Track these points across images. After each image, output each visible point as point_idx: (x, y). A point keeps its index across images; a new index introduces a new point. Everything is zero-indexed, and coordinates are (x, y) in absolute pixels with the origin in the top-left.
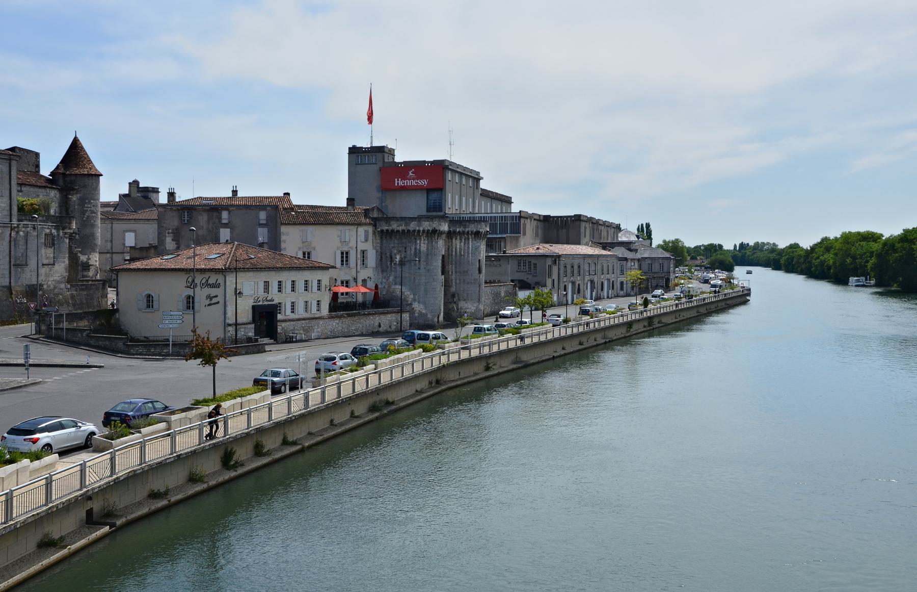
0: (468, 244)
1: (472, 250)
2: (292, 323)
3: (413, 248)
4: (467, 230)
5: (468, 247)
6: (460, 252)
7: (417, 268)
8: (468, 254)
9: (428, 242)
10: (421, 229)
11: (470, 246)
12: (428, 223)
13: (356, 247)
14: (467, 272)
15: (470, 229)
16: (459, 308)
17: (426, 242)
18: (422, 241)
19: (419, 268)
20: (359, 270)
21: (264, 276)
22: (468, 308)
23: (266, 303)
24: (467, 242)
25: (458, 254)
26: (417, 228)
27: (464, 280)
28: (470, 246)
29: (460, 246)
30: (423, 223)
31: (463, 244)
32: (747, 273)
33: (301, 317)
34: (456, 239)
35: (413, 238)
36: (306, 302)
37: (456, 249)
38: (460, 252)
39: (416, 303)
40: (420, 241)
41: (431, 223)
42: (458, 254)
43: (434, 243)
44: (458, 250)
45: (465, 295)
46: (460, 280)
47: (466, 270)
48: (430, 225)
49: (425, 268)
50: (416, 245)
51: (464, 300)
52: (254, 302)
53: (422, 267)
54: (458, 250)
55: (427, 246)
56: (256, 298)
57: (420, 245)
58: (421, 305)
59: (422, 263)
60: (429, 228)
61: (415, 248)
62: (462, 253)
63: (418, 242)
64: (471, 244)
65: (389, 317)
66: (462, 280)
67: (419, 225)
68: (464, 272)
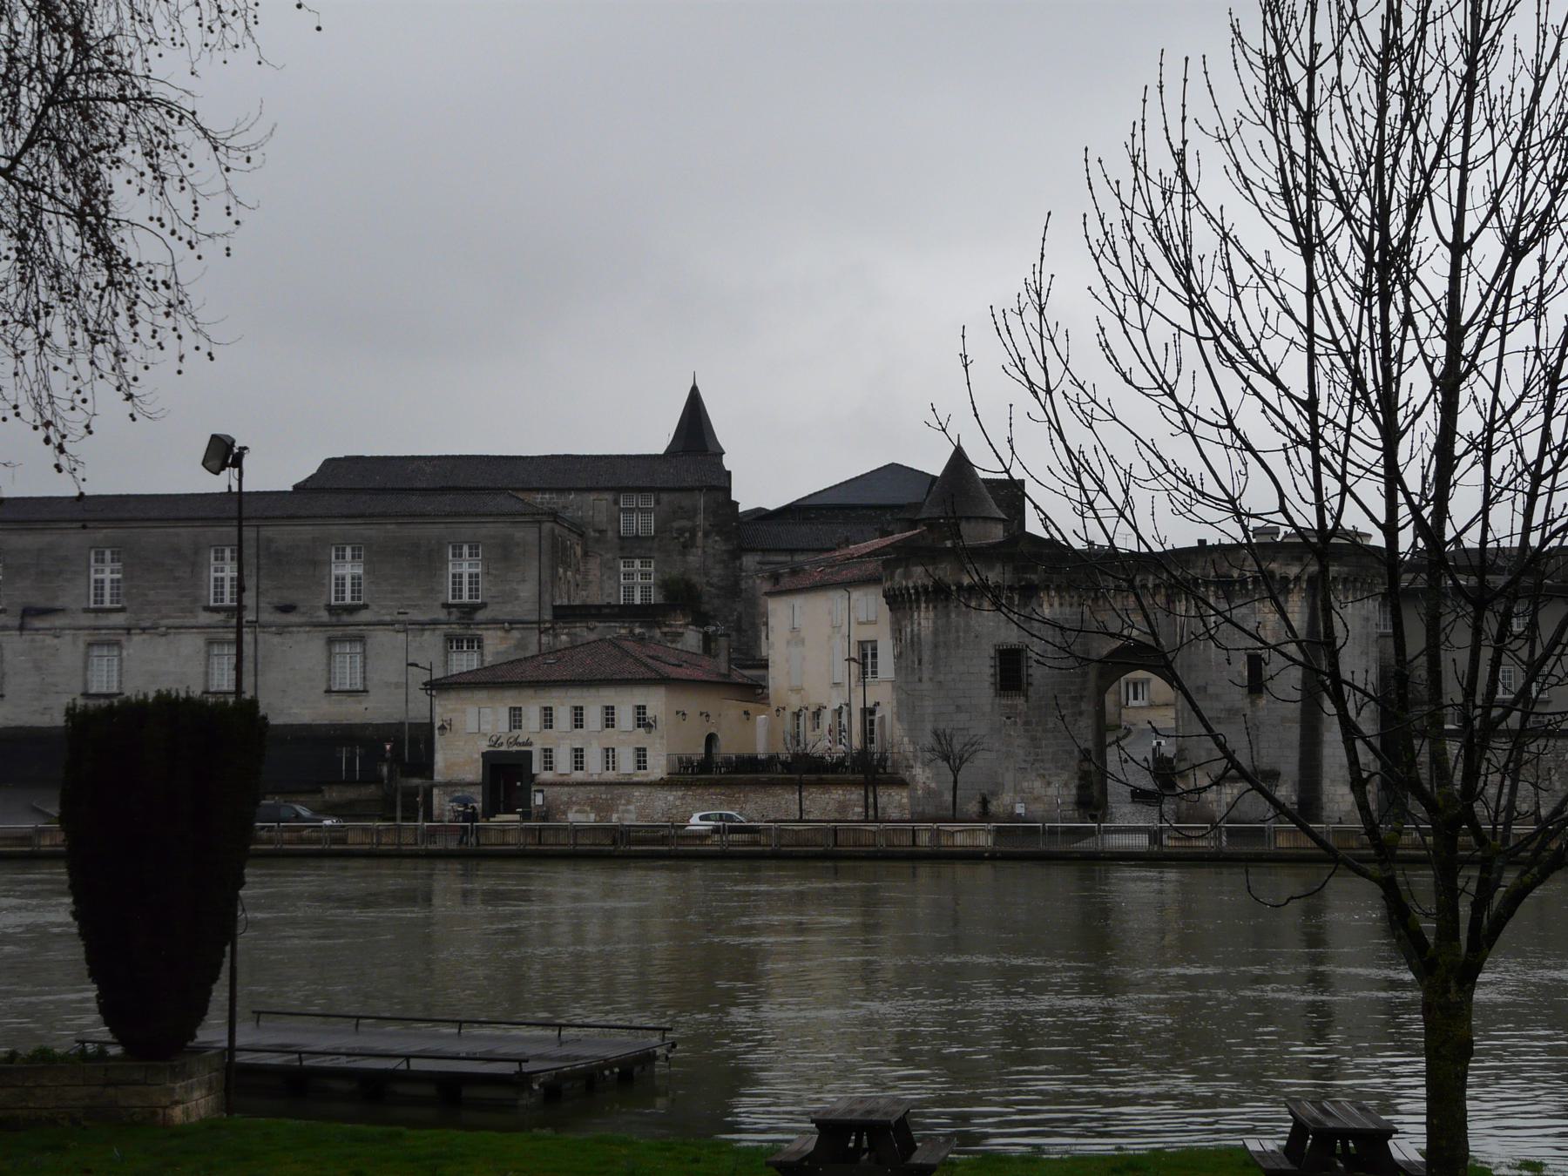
2: (566, 789)
3: (909, 630)
9: (936, 616)
10: (911, 585)
14: (1205, 688)
17: (931, 614)
18: (922, 614)
19: (920, 680)
20: (853, 685)
21: (510, 698)
23: (515, 748)
30: (914, 568)
33: (595, 778)
36: (607, 750)
39: (919, 765)
40: (919, 616)
41: (931, 569)
43: (953, 616)
49: (931, 679)
50: (912, 624)
52: (490, 746)
53: (926, 677)
55: (934, 623)
56: (494, 739)
57: (919, 624)
58: (928, 771)
61: (912, 630)
63: (916, 614)
65: (837, 794)
67: (907, 576)
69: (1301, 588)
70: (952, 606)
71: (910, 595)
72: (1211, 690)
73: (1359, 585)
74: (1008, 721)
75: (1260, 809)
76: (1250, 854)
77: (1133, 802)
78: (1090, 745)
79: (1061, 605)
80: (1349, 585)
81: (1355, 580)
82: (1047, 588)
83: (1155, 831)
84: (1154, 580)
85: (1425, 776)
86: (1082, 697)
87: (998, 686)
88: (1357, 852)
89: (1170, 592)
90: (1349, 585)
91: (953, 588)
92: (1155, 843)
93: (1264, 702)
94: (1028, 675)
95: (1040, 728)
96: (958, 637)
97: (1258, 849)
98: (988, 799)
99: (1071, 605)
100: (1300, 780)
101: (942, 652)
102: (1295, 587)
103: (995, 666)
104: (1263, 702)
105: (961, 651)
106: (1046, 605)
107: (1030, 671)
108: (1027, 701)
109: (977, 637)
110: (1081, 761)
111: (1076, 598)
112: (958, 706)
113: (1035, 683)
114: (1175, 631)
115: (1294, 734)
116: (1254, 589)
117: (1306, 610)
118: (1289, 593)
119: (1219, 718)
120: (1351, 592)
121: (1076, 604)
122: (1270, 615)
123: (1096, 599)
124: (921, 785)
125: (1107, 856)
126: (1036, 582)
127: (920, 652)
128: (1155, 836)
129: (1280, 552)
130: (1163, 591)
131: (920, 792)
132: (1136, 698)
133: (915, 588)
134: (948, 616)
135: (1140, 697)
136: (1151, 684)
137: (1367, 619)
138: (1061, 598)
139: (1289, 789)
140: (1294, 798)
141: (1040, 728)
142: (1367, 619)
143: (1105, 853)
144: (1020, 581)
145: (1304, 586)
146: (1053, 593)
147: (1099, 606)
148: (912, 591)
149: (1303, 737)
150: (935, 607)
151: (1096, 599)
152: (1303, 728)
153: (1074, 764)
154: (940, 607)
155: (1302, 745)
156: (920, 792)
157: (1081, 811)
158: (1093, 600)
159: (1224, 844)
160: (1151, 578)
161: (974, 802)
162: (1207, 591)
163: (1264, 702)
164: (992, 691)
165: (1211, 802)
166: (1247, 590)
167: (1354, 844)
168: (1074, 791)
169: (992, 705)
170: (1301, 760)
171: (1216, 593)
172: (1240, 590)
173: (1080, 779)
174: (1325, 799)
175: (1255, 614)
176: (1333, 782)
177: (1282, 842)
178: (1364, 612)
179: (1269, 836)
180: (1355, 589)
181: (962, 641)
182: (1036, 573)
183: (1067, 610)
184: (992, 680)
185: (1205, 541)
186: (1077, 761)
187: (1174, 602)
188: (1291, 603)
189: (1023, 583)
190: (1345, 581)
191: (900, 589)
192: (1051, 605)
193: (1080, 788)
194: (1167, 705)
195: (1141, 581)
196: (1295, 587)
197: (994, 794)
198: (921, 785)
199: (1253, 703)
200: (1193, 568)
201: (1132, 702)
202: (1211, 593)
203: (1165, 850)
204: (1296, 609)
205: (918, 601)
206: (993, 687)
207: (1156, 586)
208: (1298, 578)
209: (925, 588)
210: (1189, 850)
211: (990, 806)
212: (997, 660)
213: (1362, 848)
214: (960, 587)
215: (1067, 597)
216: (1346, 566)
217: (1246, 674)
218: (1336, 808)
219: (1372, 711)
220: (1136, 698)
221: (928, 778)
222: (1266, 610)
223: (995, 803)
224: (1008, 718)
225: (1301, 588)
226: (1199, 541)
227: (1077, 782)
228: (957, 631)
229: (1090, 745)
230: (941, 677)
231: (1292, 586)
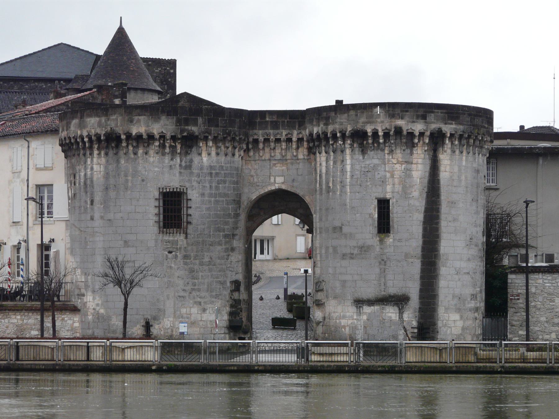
0: (343, 161)
1: (352, 176)
3: (82, 174)
4: (330, 128)
5: (343, 171)
6: (327, 183)
7: (89, 218)
8: (343, 187)
9: (107, 161)
10: (85, 134)
11: (348, 168)
12: (98, 119)
13: (28, 180)
14: (341, 228)
15: (337, 127)
16: (326, 315)
17: (103, 160)
18: (95, 160)
19: (92, 219)
20: (31, 224)
22: (344, 317)
24: (340, 158)
25: (324, 187)
26: (79, 132)
27: (335, 249)
28: (348, 168)
29: (327, 167)
30: (88, 120)
31: (331, 163)
32: (52, 185)
34: (320, 153)
35: (82, 152)
37: (321, 176)
38: (327, 183)
39: (90, 293)
40: (92, 160)
41: (103, 119)
42: (324, 187)
43: (122, 161)
44: (324, 176)
45: (338, 284)
46: (327, 248)
47: (337, 224)
48: (100, 124)
49: (102, 218)
50: (85, 169)
51: (335, 298)
53: (97, 215)
54: (324, 176)
55: (106, 168)
57: (92, 169)
58: (97, 298)
59: (97, 206)
60: (98, 131)
61: (85, 175)
62: (331, 185)
63: (89, 161)
64: (348, 162)
65: (16, 319)
66: (331, 250)
67: (81, 126)
68: (335, 228)
69: (424, 143)
70: (121, 153)
71: (84, 143)
72: (345, 230)
73: (471, 141)
74: (170, 255)
75: (386, 332)
76: (384, 366)
77: (274, 328)
78: (240, 277)
79: (218, 154)
80: (464, 142)
81: (469, 137)
82: (206, 139)
83: (303, 348)
84: (298, 134)
85: (522, 305)
86: (234, 235)
87: (162, 224)
88: (474, 365)
89: (311, 145)
90: (464, 142)
91: (123, 137)
92: (303, 357)
93: (391, 240)
94: (187, 215)
95: (197, 262)
96: (127, 181)
97: (390, 362)
98: (150, 323)
99: (226, 155)
100: (420, 308)
101: (112, 194)
102: (419, 141)
103: (159, 207)
104: (389, 240)
105: (129, 192)
106: (204, 154)
107: (190, 211)
108: (186, 238)
109: (143, 180)
110: (232, 291)
111: (230, 149)
112: (126, 242)
113: (194, 222)
114: (316, 179)
115: (416, 267)
116: (385, 142)
117: (428, 162)
118: (414, 147)
119: (353, 254)
120: (465, 146)
121: (230, 154)
122: (397, 166)
123: (247, 150)
124: (91, 311)
125: (260, 368)
126: (197, 134)
127: (92, 194)
128: (303, 352)
129: (407, 111)
130: (305, 144)
131: (90, 317)
132: (262, 252)
133: (89, 137)
134: (118, 162)
135: (266, 252)
136: (275, 240)
137: (478, 171)
138: (218, 148)
139: (411, 315)
140: (415, 324)
141: (197, 262)
142: (478, 171)
143: (259, 366)
144: (182, 131)
145: (427, 141)
146: (210, 143)
147: (250, 157)
148: (86, 140)
149: (423, 271)
150: (106, 154)
151: (247, 150)
152: (423, 263)
153: (226, 293)
154: (111, 153)
155: (422, 278)
156: (90, 317)
157: (232, 334)
158: (245, 151)
159: (361, 359)
160: (295, 132)
161: (138, 326)
162: (344, 143)
163: (391, 240)
164: (156, 229)
165: (344, 327)
166: (379, 143)
167: (472, 358)
168: (226, 317)
169: (156, 241)
170: (421, 291)
171: (352, 146)
172: (373, 143)
173: (232, 306)
174: (440, 324)
175: (385, 164)
176: (447, 309)
177: (411, 357)
178: (475, 165)
179: (401, 350)
180: (468, 145)
181: (130, 184)
182: (196, 124)
183: (222, 158)
184: (156, 219)
185: (342, 101)
186: (229, 291)
187: (314, 154)
188: (415, 156)
189: (185, 134)
190: (461, 137)
191: (75, 138)
192: (209, 154)
193: (231, 314)
194: (288, 259)
195: (286, 135)
196: (419, 141)
197: (155, 318)
198: (91, 311)
199: (381, 241)
200: (333, 124)
201: (259, 256)
202: (347, 146)
203: (310, 364)
204: (420, 161)
205: (91, 148)
206: (157, 225)
207: (300, 140)
208: (422, 134)
209: (98, 136)
210: (333, 364)
211: (152, 329)
212: (161, 201)
213: (478, 362)
214: (129, 136)
215: (223, 148)
216: (461, 124)
217: (376, 216)
218: (449, 332)
219: (480, 250)
220: (262, 252)
221: (98, 305)
222: (395, 161)
223: (157, 327)
224: (170, 252)
225: (424, 143)
226: (337, 102)
227: (228, 309)
228: (126, 176)
229: (240, 277)
230: (111, 216)
231: (416, 141)
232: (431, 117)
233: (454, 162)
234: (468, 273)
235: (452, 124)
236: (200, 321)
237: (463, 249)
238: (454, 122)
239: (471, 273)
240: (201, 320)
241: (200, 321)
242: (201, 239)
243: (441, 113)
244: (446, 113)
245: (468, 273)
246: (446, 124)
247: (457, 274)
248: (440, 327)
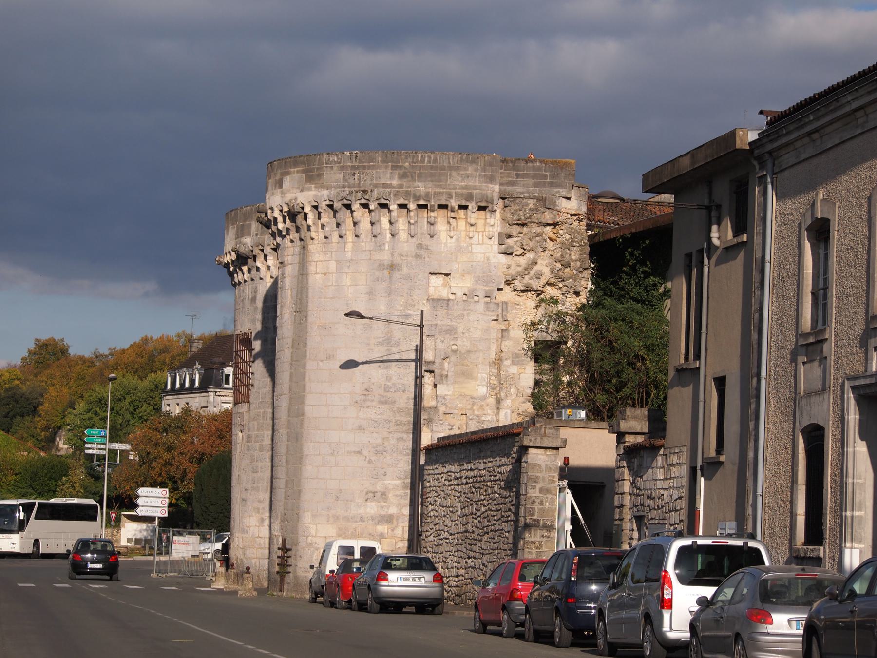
216: (323, 187)
232: (287, 183)
233: (330, 254)
234: (359, 453)
235: (309, 189)
236: (257, 537)
237: (345, 408)
238: (313, 186)
239: (365, 452)
240: (259, 537)
241: (257, 537)
242: (262, 411)
243: (298, 172)
244: (303, 171)
245: (359, 453)
246: (302, 191)
247: (332, 454)
248: (303, 548)
